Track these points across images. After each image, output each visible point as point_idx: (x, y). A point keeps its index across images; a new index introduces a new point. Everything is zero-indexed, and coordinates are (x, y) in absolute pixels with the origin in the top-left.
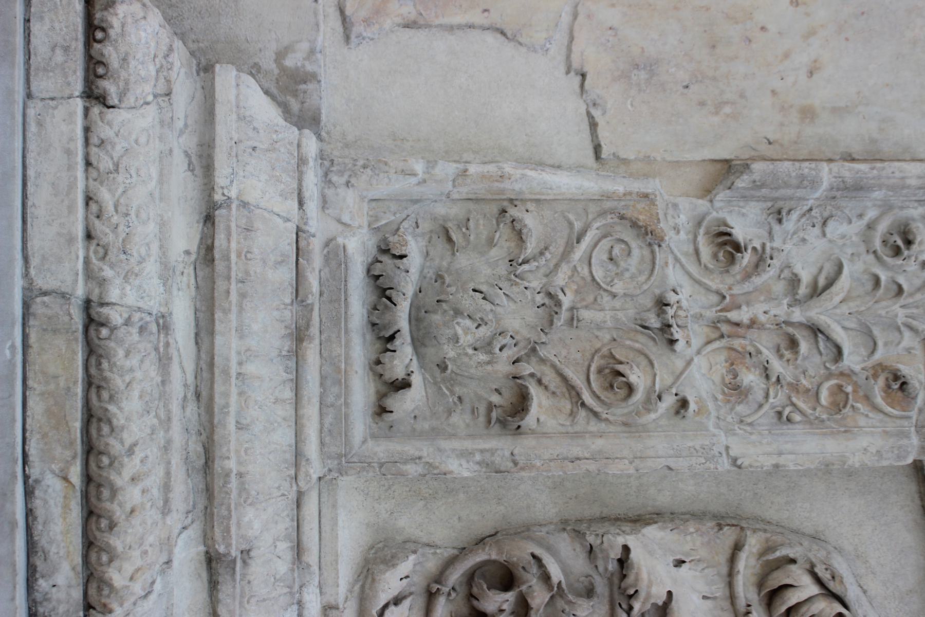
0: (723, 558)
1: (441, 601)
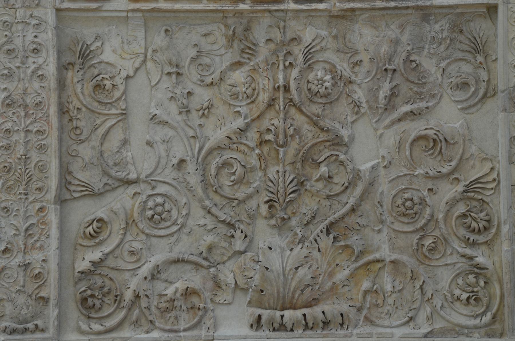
0: (84, 248)
1: (90, 315)
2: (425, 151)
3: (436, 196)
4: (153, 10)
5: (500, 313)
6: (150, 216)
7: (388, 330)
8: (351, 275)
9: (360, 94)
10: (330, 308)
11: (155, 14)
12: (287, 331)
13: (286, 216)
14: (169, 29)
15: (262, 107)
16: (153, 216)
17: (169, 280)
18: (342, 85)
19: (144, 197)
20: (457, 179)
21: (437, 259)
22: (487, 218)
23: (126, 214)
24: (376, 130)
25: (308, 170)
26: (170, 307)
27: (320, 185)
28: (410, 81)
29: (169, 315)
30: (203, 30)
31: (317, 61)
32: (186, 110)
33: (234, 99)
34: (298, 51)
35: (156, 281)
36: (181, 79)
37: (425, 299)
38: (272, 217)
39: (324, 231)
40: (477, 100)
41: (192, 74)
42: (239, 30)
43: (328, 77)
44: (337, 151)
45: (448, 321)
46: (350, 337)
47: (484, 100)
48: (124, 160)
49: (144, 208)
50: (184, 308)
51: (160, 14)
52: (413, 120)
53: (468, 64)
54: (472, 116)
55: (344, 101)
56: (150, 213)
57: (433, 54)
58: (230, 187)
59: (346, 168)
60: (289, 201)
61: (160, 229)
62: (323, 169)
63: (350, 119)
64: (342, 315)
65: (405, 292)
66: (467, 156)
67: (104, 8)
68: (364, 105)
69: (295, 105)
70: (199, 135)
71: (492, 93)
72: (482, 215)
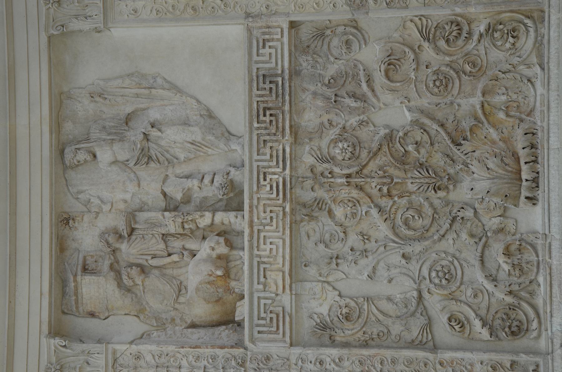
0: (472, 332)
1: (525, 329)
2: (397, 71)
3: (432, 62)
4: (290, 275)
5: (524, 13)
6: (447, 282)
7: (538, 98)
8: (493, 127)
10: (520, 143)
11: (293, 273)
12: (538, 177)
13: (447, 177)
14: (304, 263)
15: (362, 194)
16: (446, 279)
17: (497, 268)
18: (346, 134)
19: (432, 286)
20: (419, 47)
21: (482, 61)
22: (449, 24)
23: (444, 300)
24: (380, 108)
25: (410, 160)
26: (518, 267)
27: (423, 151)
28: (344, 84)
29: (526, 268)
31: (328, 153)
32: (365, 253)
33: (356, 216)
34: (321, 167)
35: (498, 278)
36: (341, 256)
37: (513, 69)
38: (447, 187)
39: (458, 147)
40: (359, 34)
41: (337, 247)
42: (304, 211)
43: (340, 145)
44: (396, 138)
45: (531, 52)
46: (543, 128)
47: (359, 28)
48: (403, 300)
49: (441, 286)
50: (519, 257)
51: (294, 271)
52: (374, 81)
53: (333, 41)
54: (371, 37)
55: (358, 133)
56: (444, 281)
57: (324, 67)
58: (424, 219)
59: (410, 131)
60: (435, 175)
61: (456, 274)
62: (410, 148)
63: (372, 128)
64: (526, 134)
65: (507, 86)
66: (401, 40)
67: (290, 312)
68: (361, 117)
69: (361, 170)
70: (384, 243)
71: (354, 22)
72: (447, 28)
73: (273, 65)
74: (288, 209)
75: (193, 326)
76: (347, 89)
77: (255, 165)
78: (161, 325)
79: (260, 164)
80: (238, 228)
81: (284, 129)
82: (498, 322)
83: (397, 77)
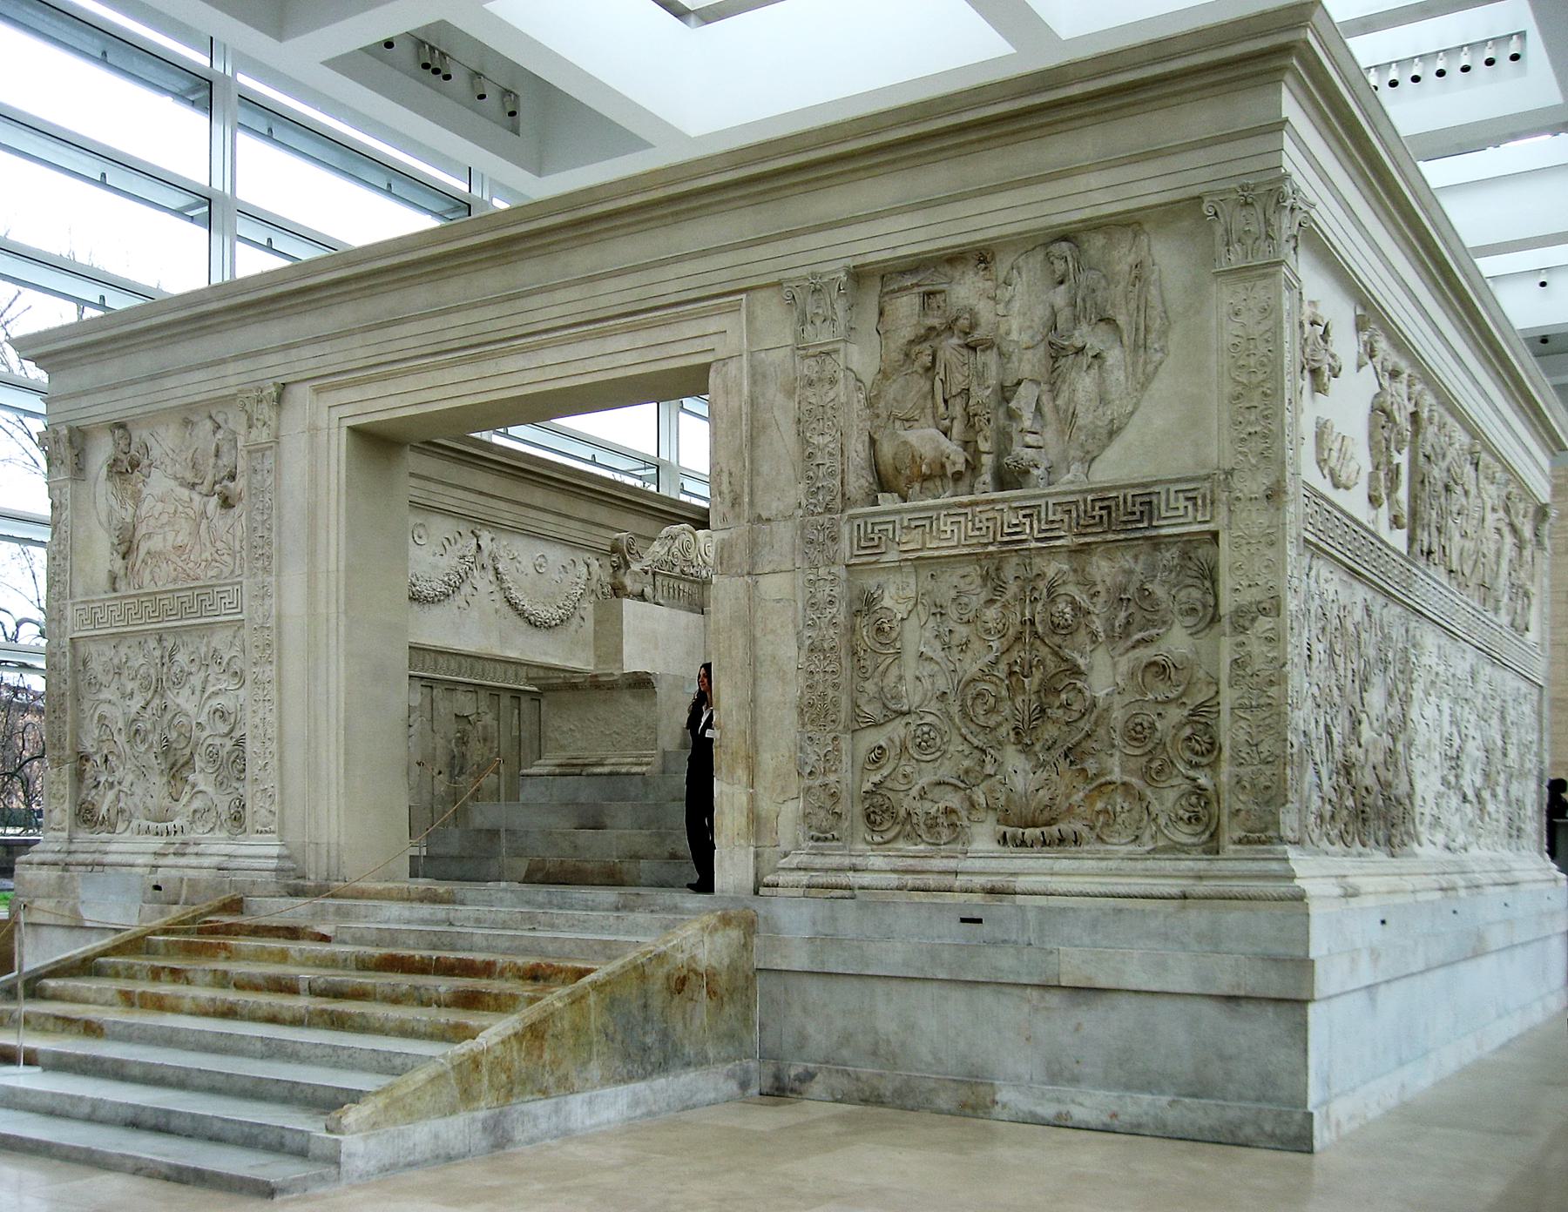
9: (1098, 625)
10: (1066, 827)
19: (913, 727)
26: (932, 825)
27: (1060, 712)
30: (961, 572)
32: (947, 647)
34: (1042, 585)
41: (953, 612)
42: (992, 569)
55: (1083, 631)
62: (1063, 696)
63: (1088, 649)
72: (1206, 738)
73: (1164, 514)
74: (991, 548)
75: (873, 442)
76: (1137, 614)
77: (1042, 502)
78: (870, 403)
79: (1043, 509)
80: (979, 486)
81: (1085, 535)
82: (878, 800)
83: (1149, 678)
